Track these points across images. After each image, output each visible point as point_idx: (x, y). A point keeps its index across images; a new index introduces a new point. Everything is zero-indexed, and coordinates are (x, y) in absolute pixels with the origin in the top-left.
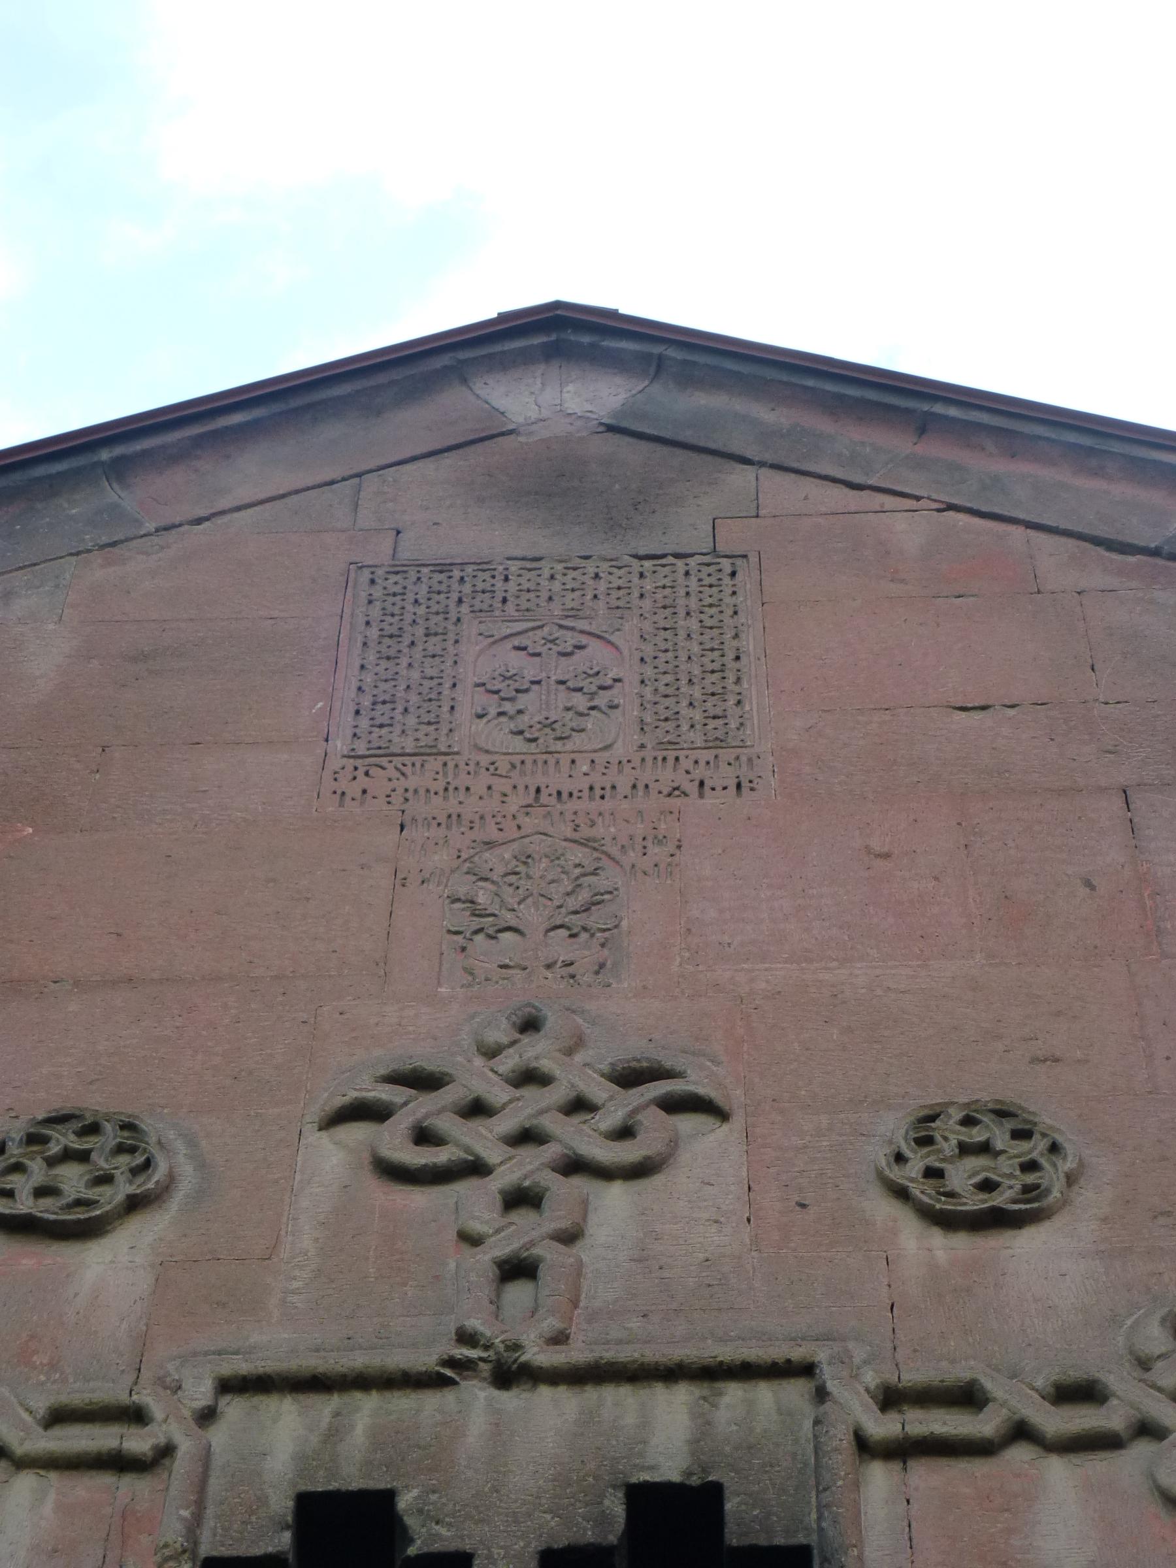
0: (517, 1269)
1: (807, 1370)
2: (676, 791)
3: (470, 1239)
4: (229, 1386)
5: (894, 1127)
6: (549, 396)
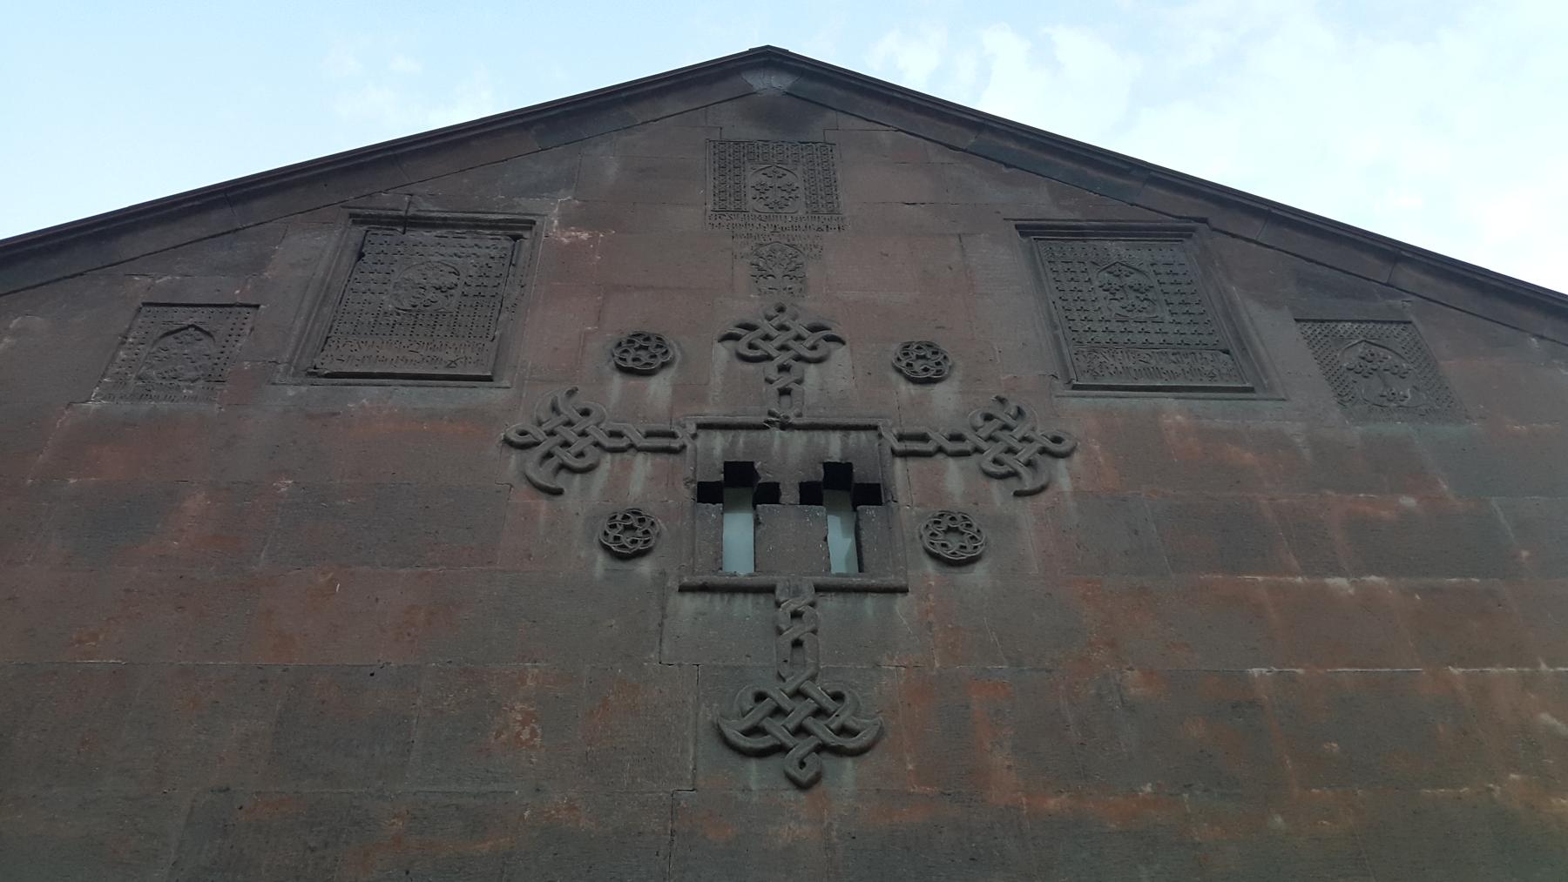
0: (785, 392)
1: (875, 428)
2: (819, 229)
3: (770, 382)
4: (700, 426)
5: (896, 348)
6: (766, 79)
